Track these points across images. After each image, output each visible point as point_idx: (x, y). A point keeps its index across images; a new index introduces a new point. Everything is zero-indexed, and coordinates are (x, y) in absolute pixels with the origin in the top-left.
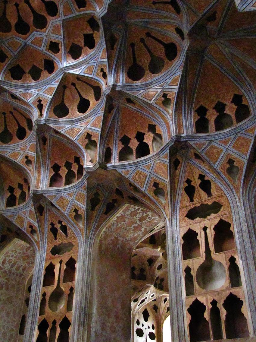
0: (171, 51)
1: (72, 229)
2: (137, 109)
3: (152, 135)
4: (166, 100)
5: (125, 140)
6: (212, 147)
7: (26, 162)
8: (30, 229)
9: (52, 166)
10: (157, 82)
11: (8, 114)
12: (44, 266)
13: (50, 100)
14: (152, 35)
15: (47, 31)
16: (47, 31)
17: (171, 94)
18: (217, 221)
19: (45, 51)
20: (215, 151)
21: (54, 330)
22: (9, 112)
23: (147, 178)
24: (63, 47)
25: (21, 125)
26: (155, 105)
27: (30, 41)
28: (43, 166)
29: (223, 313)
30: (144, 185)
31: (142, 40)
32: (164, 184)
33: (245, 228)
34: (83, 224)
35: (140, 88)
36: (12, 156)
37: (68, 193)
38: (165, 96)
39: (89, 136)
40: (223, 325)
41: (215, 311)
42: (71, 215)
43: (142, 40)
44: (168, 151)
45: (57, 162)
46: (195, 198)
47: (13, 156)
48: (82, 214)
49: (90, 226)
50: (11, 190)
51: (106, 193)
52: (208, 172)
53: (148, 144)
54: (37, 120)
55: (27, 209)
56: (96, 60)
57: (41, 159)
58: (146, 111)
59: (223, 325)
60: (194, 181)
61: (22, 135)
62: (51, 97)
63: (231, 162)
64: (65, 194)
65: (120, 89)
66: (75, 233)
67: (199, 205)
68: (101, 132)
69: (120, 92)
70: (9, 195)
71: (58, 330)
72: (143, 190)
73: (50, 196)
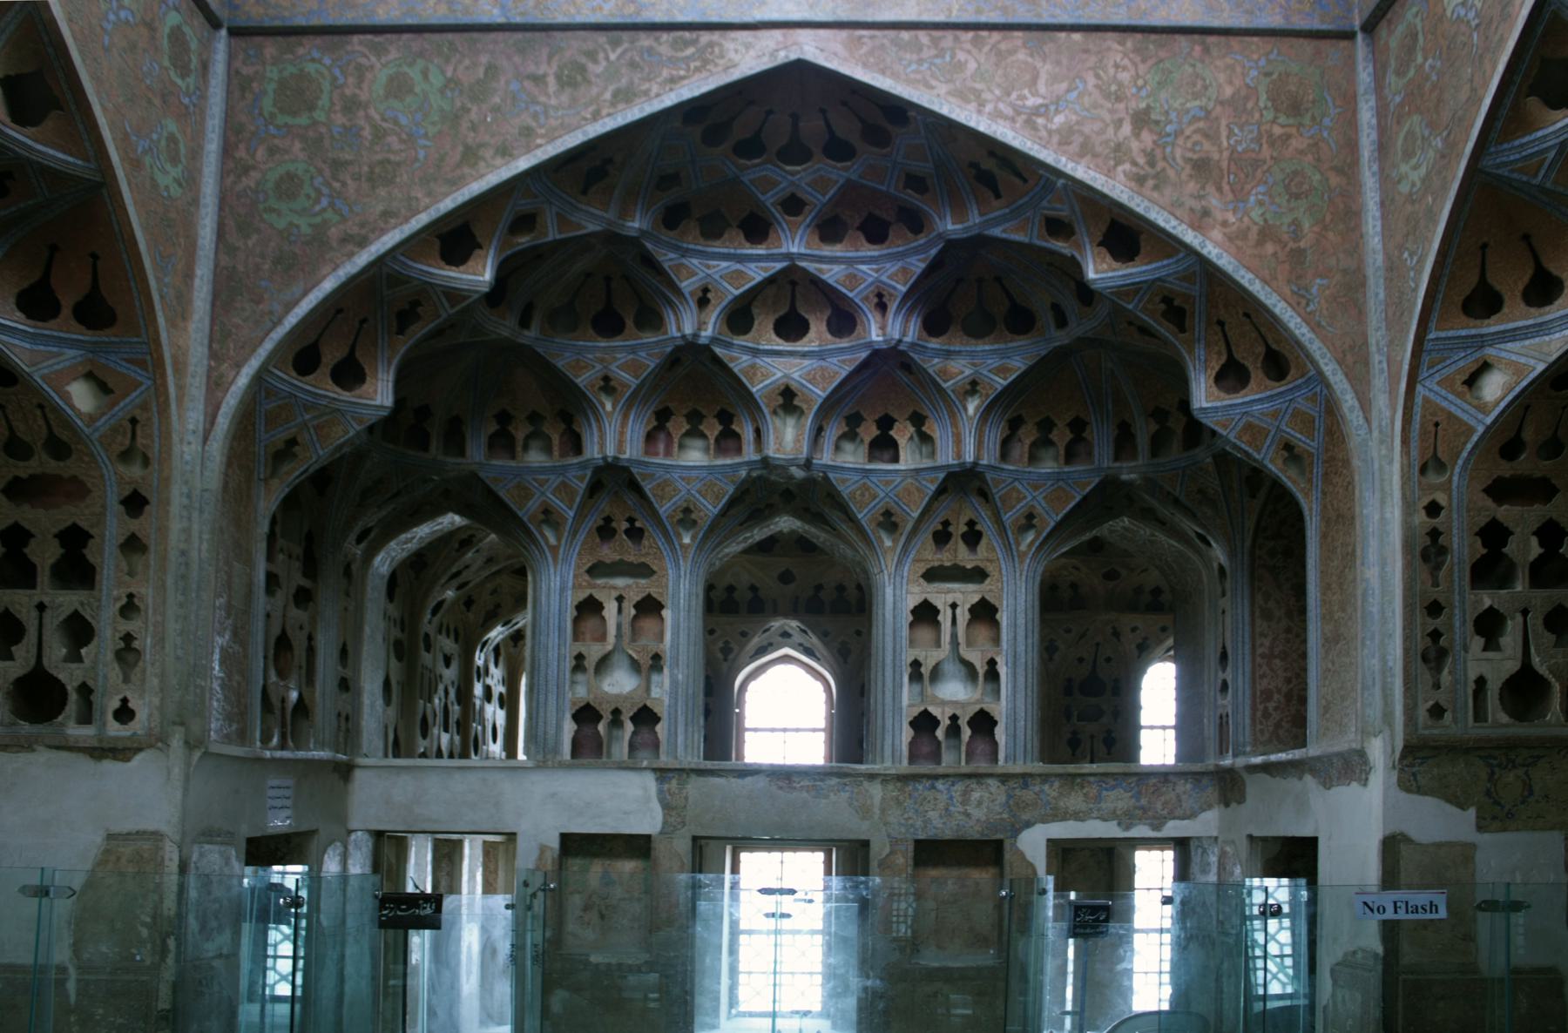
3: (912, 429)
4: (973, 387)
5: (854, 421)
10: (972, 354)
13: (730, 297)
34: (693, 538)
35: (937, 353)
44: (942, 476)
45: (671, 405)
54: (696, 336)
56: (877, 271)
61: (609, 325)
62: (737, 292)
63: (1030, 516)
67: (948, 564)
69: (903, 353)
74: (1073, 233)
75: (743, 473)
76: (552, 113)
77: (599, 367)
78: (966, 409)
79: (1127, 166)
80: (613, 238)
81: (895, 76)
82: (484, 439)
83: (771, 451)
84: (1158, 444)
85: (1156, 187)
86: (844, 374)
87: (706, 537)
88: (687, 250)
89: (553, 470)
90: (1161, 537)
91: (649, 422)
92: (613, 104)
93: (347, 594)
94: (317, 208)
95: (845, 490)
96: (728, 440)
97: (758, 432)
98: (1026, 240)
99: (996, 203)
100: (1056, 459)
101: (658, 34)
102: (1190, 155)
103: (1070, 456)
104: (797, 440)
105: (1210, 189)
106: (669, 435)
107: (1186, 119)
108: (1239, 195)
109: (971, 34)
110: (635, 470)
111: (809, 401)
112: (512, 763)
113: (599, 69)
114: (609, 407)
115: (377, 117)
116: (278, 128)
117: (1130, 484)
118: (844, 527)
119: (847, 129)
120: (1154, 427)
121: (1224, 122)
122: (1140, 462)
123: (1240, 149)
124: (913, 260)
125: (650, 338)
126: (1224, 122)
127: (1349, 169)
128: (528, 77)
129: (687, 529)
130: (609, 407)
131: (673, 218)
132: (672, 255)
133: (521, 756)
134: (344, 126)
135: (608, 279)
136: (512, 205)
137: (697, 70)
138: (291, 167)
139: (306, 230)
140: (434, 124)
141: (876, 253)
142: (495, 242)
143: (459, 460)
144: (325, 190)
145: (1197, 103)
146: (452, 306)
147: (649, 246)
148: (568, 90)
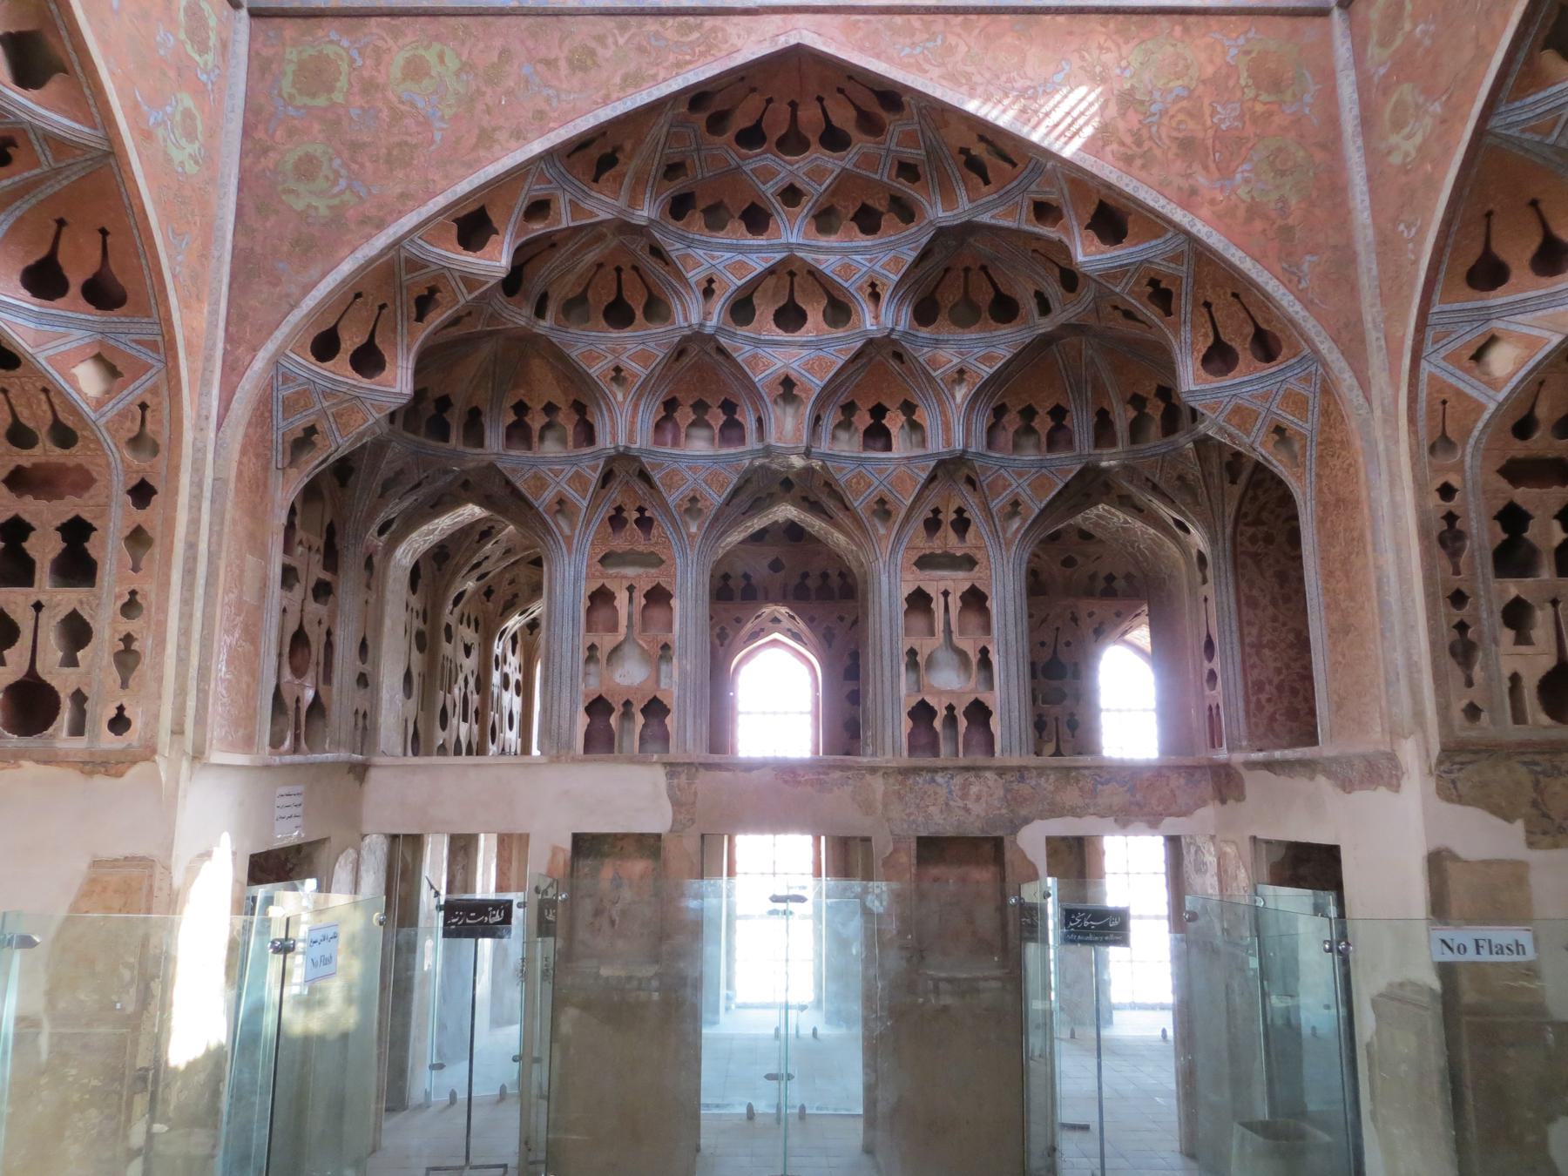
0: (1005, 309)
5: (849, 409)
7: (613, 379)
12: (585, 590)
13: (734, 288)
18: (966, 586)
20: (1001, 482)
21: (627, 714)
29: (963, 723)
31: (967, 270)
33: (1010, 609)
34: (699, 529)
38: (961, 372)
40: (961, 739)
41: (951, 719)
44: (933, 464)
50: (521, 408)
54: (702, 325)
55: (567, 467)
56: (870, 261)
59: (961, 739)
62: (739, 283)
69: (894, 342)
70: (511, 418)
71: (640, 720)
74: (1060, 217)
75: (747, 462)
76: (563, 96)
79: (1115, 146)
80: (625, 228)
81: (890, 60)
82: (502, 430)
83: (772, 439)
84: (1137, 430)
85: (1143, 167)
86: (841, 363)
87: (712, 525)
89: (567, 461)
90: (1138, 525)
92: (622, 89)
93: (368, 586)
94: (336, 190)
95: (842, 478)
96: (732, 430)
97: (760, 420)
99: (985, 189)
100: (1038, 447)
101: (664, 19)
102: (1175, 134)
103: (1052, 445)
104: (797, 429)
105: (1196, 167)
106: (676, 425)
107: (1170, 98)
108: (1225, 172)
109: (961, 18)
111: (807, 391)
112: (526, 759)
113: (608, 53)
114: (620, 397)
115: (394, 99)
116: (297, 108)
117: (1107, 470)
118: (841, 516)
119: (843, 117)
120: (1132, 414)
121: (1206, 102)
122: (1120, 448)
123: (1223, 127)
124: (904, 249)
125: (658, 329)
126: (1206, 102)
127: (1332, 144)
128: (540, 61)
129: (694, 519)
130: (620, 397)
131: (679, 207)
132: (678, 246)
133: (535, 752)
134: (362, 107)
135: (619, 270)
136: (529, 192)
137: (702, 54)
138: (310, 149)
139: (323, 211)
140: (450, 106)
142: (510, 228)
143: (479, 451)
144: (343, 172)
145: (1180, 82)
146: (470, 292)
147: (657, 235)
148: (580, 74)
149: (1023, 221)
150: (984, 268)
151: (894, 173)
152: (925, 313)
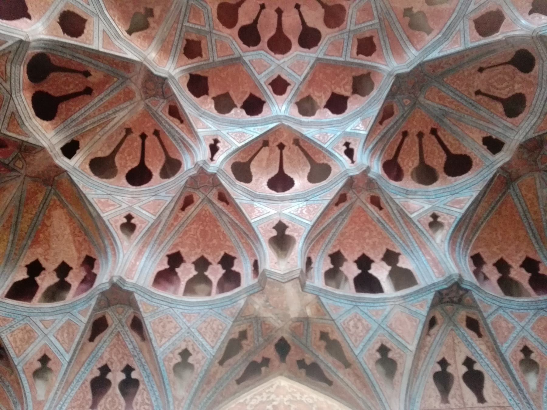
0: (458, 165)
1: (151, 393)
2: (380, 218)
3: (389, 268)
5: (337, 258)
6: (500, 317)
7: (123, 226)
8: (38, 365)
9: (169, 253)
11: (136, 135)
13: (234, 148)
14: (439, 133)
15: (282, 61)
16: (282, 61)
17: (448, 217)
19: (262, 83)
20: (503, 324)
22: (139, 134)
23: (371, 333)
24: (293, 92)
25: (147, 164)
26: (417, 223)
27: (250, 58)
28: (153, 245)
30: (359, 344)
32: (402, 353)
36: (100, 202)
37: (186, 311)
38: (435, 217)
39: (281, 227)
42: (170, 359)
43: (420, 135)
44: (430, 297)
45: (184, 251)
46: (452, 398)
47: (103, 204)
48: (196, 366)
49: (200, 397)
50: (35, 268)
51: (260, 339)
52: (483, 356)
53: (379, 278)
54: (205, 162)
55: (60, 317)
57: (158, 231)
58: (395, 227)
60: (454, 366)
61: (139, 176)
64: (178, 311)
65: (374, 177)
66: (155, 404)
68: (313, 226)
70: (22, 275)
72: (357, 352)
73: (145, 304)
75: (242, 302)
77: (124, 206)
78: (434, 239)
88: (204, 113)
91: (161, 263)
97: (256, 265)
98: (462, 48)
99: (428, 38)
110: (138, 297)
118: (340, 375)
135: (143, 136)
141: (340, 118)
149: (465, 39)
150: (434, 132)
151: (355, 51)
152: (393, 169)
